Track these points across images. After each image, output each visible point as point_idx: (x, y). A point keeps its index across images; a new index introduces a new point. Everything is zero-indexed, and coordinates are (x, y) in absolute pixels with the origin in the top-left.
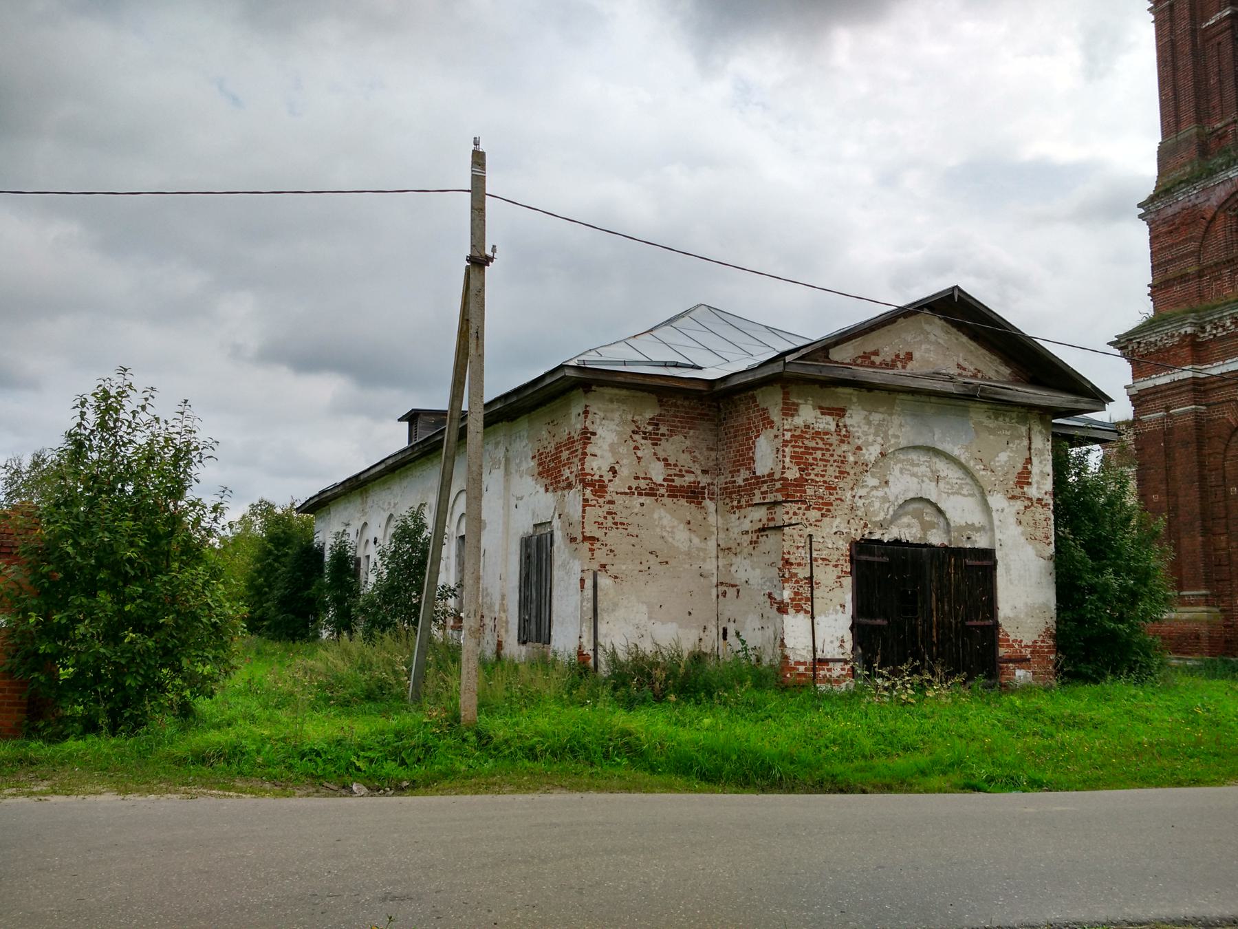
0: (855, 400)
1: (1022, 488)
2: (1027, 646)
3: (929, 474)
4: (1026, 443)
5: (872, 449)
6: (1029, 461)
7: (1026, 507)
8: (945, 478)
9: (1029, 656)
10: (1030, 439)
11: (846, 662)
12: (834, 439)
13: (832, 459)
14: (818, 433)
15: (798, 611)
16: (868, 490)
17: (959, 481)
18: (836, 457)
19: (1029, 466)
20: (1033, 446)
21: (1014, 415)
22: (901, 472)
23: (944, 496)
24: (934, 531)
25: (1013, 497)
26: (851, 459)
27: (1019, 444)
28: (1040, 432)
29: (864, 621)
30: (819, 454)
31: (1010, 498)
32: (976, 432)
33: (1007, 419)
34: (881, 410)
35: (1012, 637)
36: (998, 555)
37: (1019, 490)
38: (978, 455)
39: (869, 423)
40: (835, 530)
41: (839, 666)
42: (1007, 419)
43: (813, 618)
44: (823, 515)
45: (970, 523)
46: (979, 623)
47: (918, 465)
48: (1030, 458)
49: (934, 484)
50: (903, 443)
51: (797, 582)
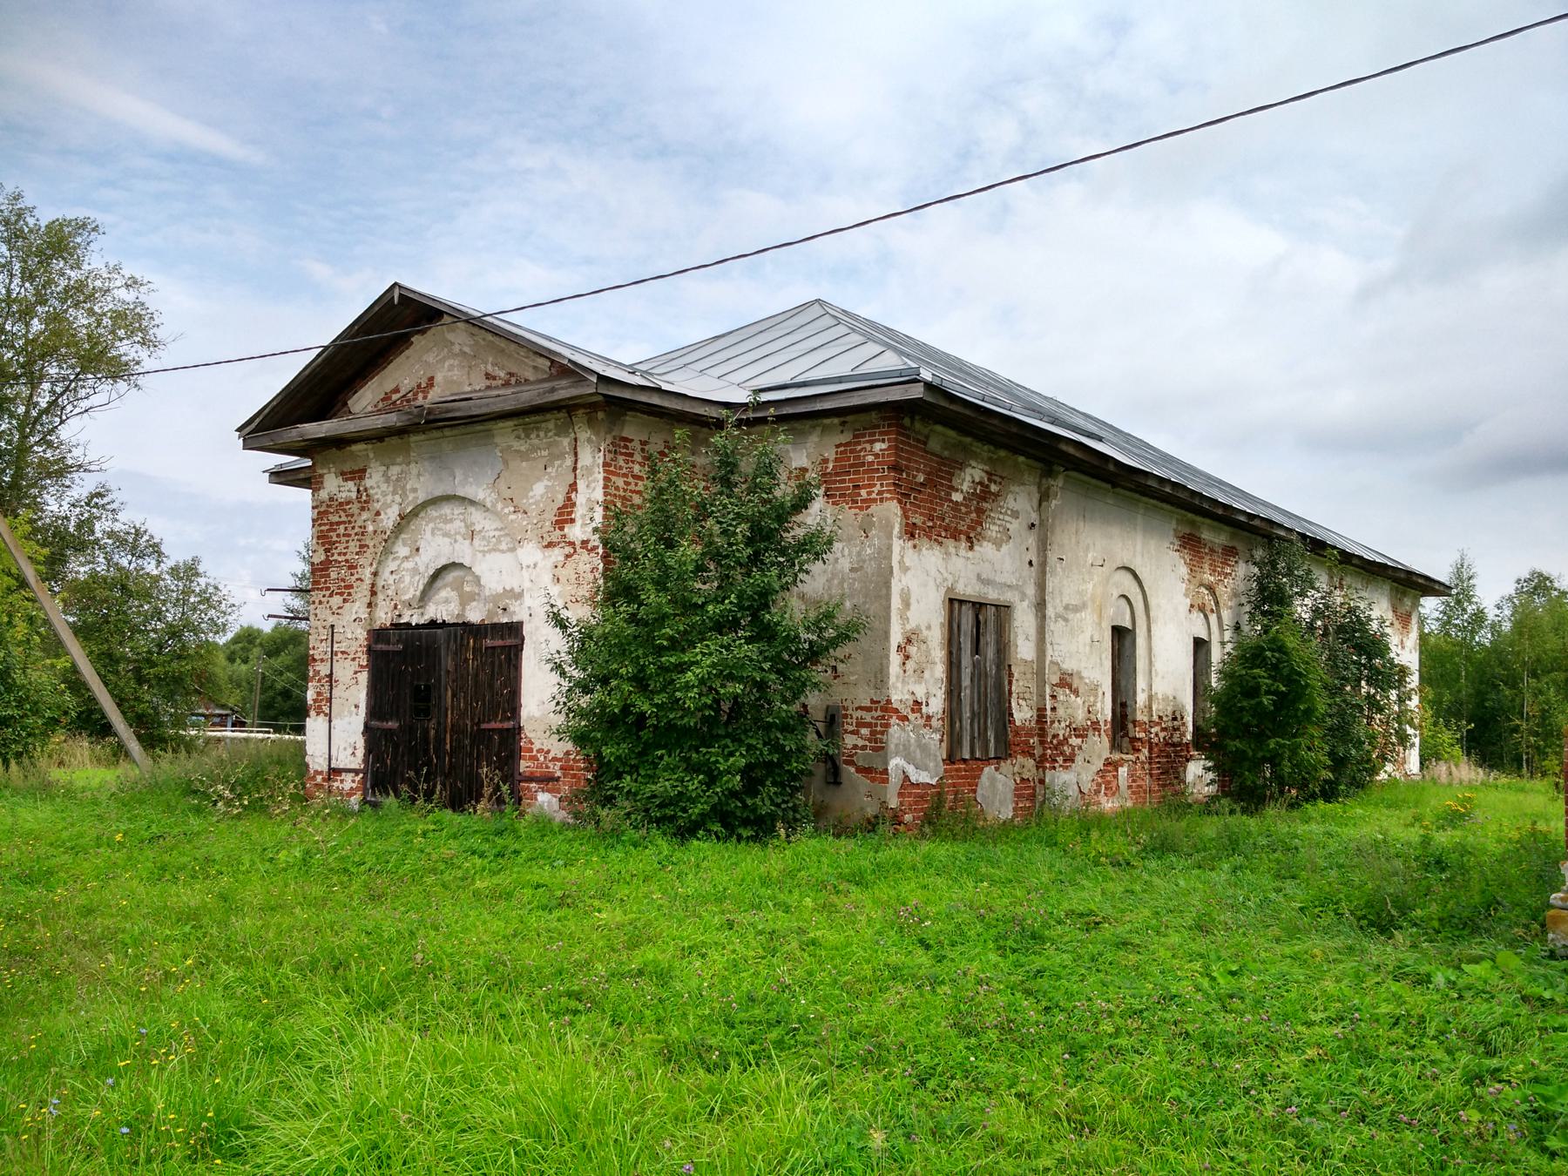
0: (371, 455)
1: (562, 529)
2: (555, 759)
3: (463, 530)
4: (569, 462)
5: (389, 511)
6: (573, 487)
7: (568, 556)
8: (480, 531)
9: (558, 774)
10: (576, 454)
11: (356, 772)
12: (355, 508)
13: (353, 532)
14: (341, 504)
15: (318, 714)
16: (398, 562)
17: (497, 533)
18: (357, 530)
19: (573, 496)
20: (579, 465)
21: (551, 425)
22: (433, 534)
23: (479, 555)
24: (474, 604)
25: (550, 545)
26: (370, 528)
27: (560, 466)
28: (589, 440)
29: (374, 723)
30: (341, 529)
31: (546, 547)
32: (506, 462)
33: (542, 434)
34: (399, 460)
35: (537, 746)
36: (526, 630)
37: (558, 532)
38: (508, 494)
39: (388, 480)
40: (354, 617)
41: (349, 777)
42: (542, 434)
43: (330, 721)
44: (345, 601)
45: (508, 588)
46: (497, 725)
47: (451, 521)
48: (575, 483)
49: (467, 542)
50: (422, 497)
51: (319, 681)
